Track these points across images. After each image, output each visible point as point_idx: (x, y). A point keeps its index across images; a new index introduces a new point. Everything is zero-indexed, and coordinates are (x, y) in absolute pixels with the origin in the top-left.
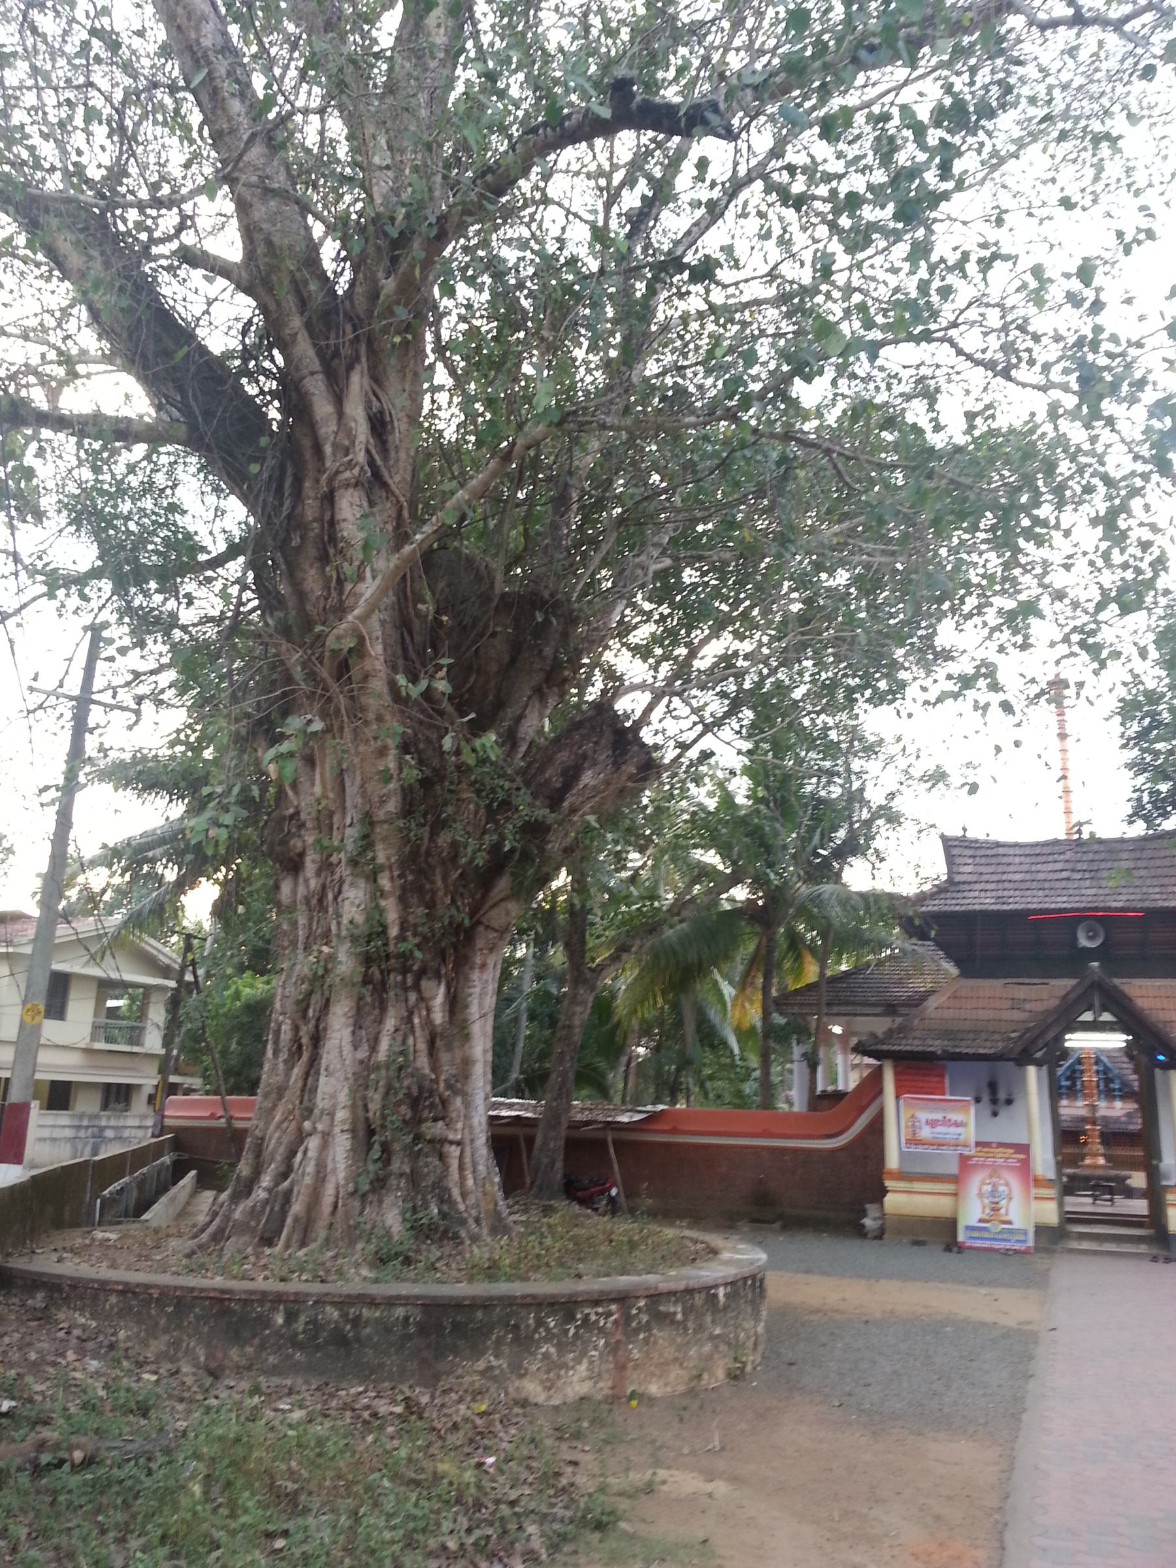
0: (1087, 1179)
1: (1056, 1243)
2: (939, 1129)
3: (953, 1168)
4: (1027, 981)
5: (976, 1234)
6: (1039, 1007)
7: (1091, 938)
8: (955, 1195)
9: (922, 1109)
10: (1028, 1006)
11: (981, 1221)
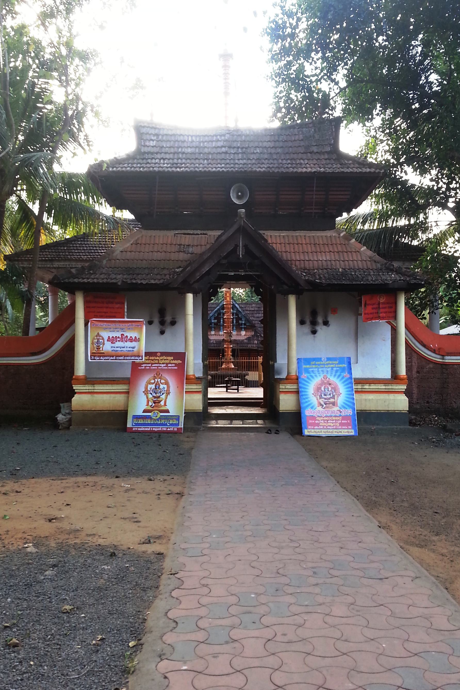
0: (223, 377)
1: (200, 424)
2: (118, 344)
3: (128, 374)
4: (191, 232)
5: (141, 421)
6: (198, 250)
7: (239, 198)
8: (128, 393)
9: (105, 329)
10: (191, 250)
11: (145, 411)
